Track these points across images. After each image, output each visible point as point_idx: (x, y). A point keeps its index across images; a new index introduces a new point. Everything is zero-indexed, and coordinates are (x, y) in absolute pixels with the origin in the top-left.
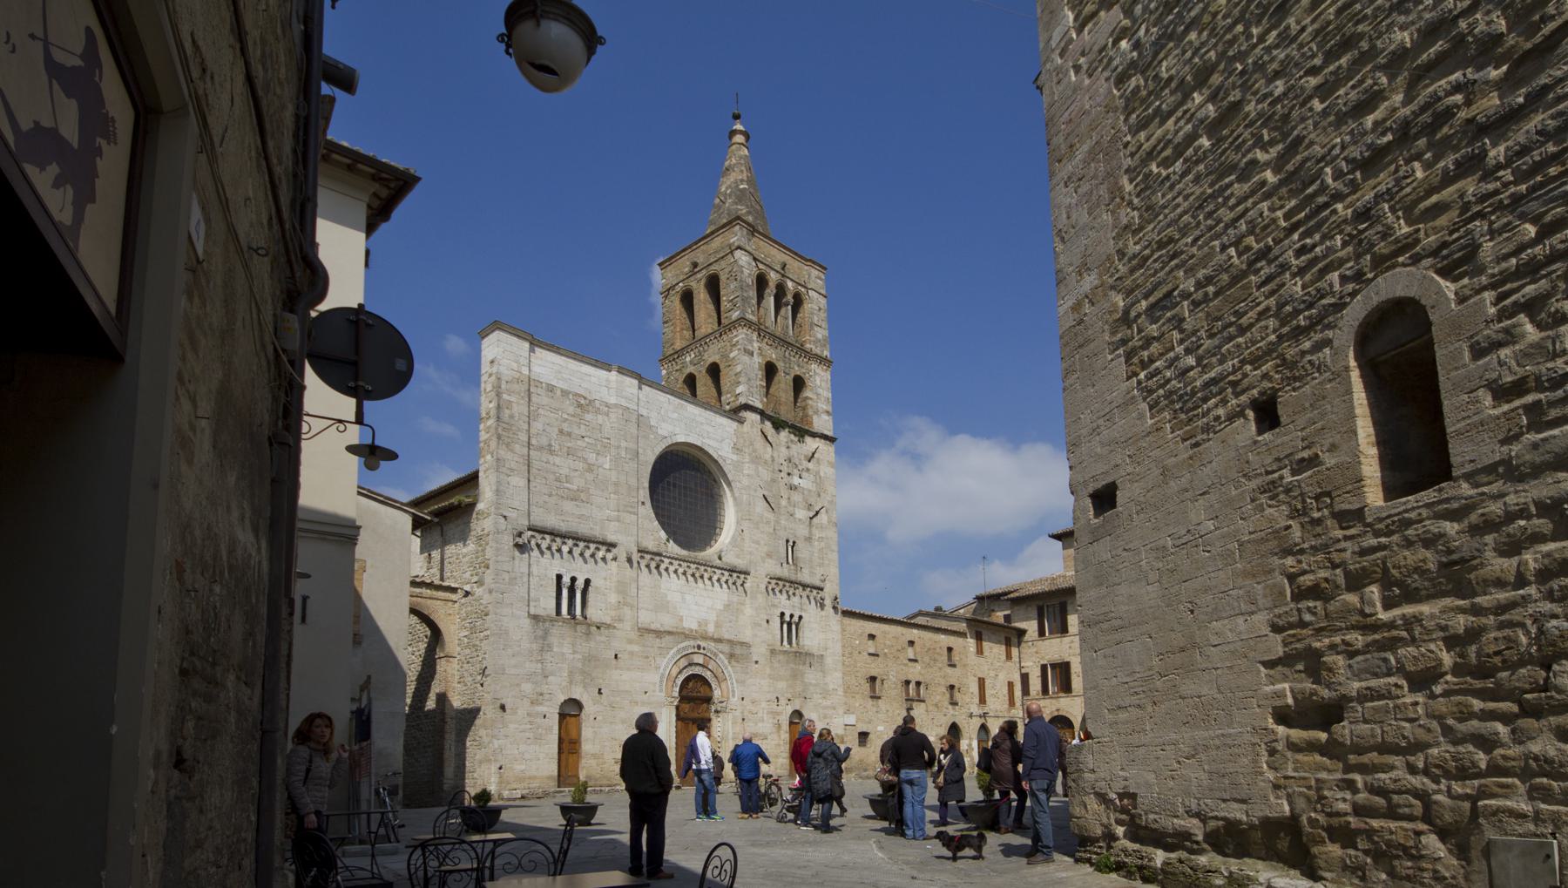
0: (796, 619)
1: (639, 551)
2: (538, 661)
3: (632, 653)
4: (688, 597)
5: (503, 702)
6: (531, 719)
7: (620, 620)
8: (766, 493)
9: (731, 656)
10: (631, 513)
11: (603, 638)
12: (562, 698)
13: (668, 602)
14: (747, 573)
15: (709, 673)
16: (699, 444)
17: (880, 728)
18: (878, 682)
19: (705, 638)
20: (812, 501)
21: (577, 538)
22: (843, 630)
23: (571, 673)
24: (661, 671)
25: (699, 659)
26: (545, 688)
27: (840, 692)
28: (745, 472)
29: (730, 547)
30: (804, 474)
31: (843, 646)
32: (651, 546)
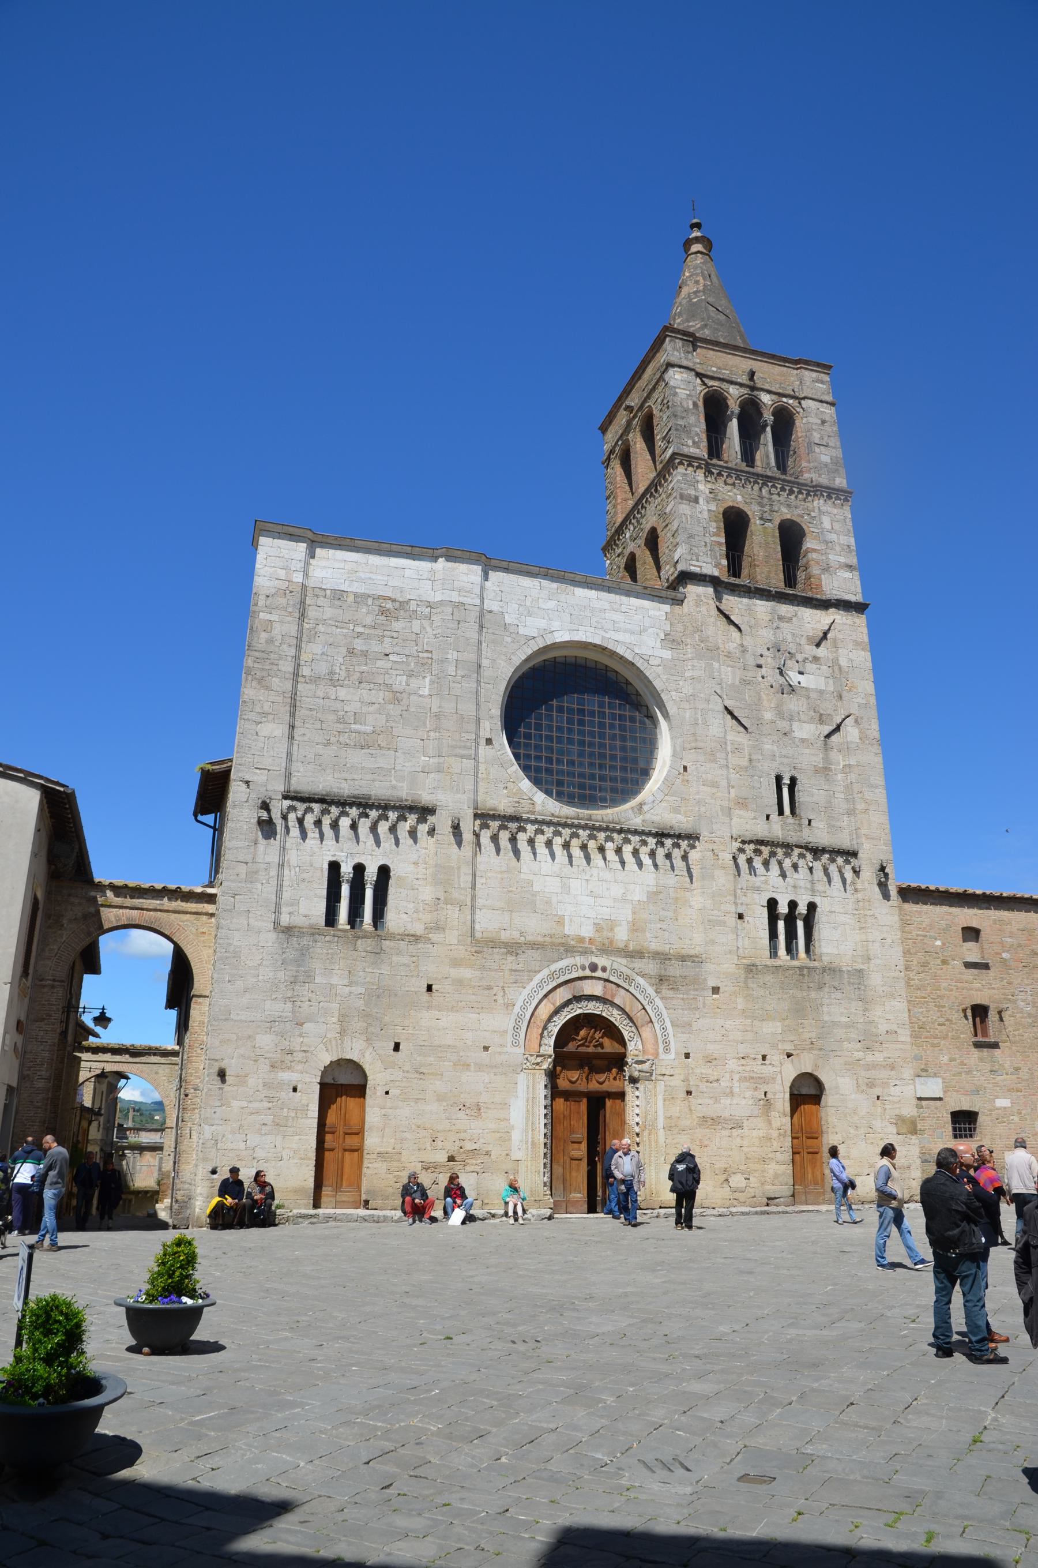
0: (802, 909)
1: (476, 816)
2: (286, 999)
3: (460, 983)
4: (575, 885)
5: (223, 1065)
6: (271, 1093)
7: (438, 928)
8: (729, 703)
9: (661, 980)
10: (462, 757)
11: (405, 960)
12: (326, 1059)
13: (535, 894)
14: (692, 838)
15: (615, 1012)
16: (597, 641)
17: (1003, 1103)
18: (993, 1016)
19: (608, 949)
20: (826, 707)
21: (364, 804)
22: (905, 923)
23: (344, 1019)
24: (517, 1009)
26: (296, 1043)
27: (905, 1036)
28: (688, 674)
29: (660, 796)
30: (810, 667)
31: (906, 952)
32: (503, 804)
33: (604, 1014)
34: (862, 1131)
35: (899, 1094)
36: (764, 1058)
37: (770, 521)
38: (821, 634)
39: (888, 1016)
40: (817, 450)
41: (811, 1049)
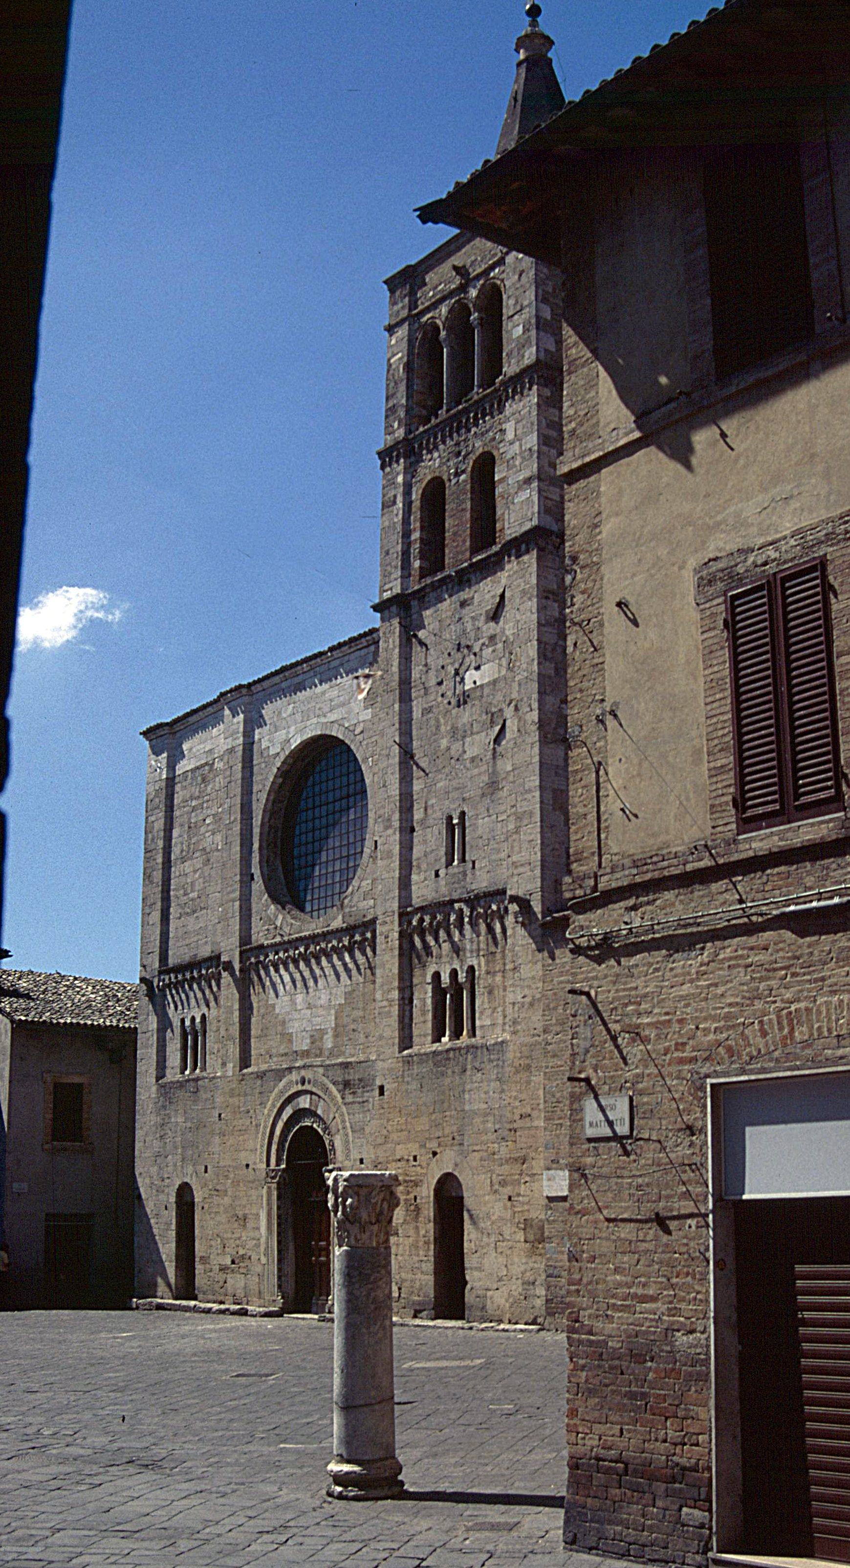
12: (178, 1183)
25: (304, 1102)
33: (315, 1126)
34: (493, 1239)
35: (529, 1193)
36: (415, 1159)
37: (463, 472)
38: (498, 600)
39: (523, 1096)
40: (510, 324)
41: (452, 1145)
